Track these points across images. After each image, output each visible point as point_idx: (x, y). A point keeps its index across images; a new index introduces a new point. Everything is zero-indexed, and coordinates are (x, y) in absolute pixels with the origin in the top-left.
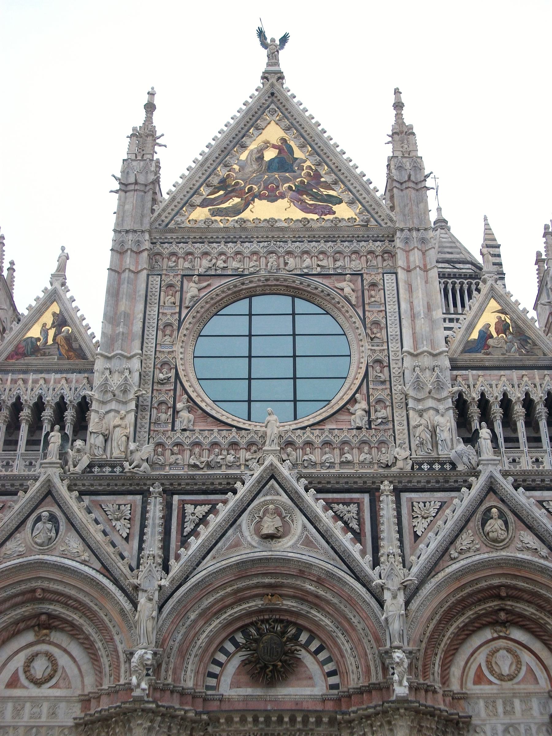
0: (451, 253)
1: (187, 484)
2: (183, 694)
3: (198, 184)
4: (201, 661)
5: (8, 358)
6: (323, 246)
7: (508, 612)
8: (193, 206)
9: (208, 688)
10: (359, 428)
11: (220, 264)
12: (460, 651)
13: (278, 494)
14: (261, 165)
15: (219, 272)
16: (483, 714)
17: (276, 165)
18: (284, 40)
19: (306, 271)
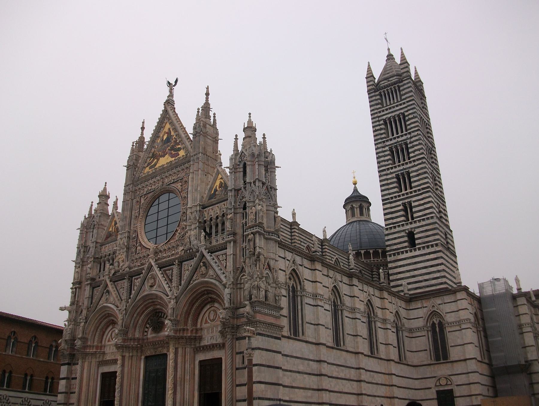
0: (388, 73)
1: (134, 273)
2: (134, 339)
3: (146, 158)
4: (142, 328)
5: (105, 240)
6: (174, 171)
7: (211, 298)
8: (145, 168)
9: (145, 336)
10: (177, 240)
11: (150, 188)
12: (201, 313)
13: (154, 271)
14: (162, 143)
15: (149, 192)
16: (206, 334)
17: (166, 140)
18: (176, 81)
19: (170, 182)
